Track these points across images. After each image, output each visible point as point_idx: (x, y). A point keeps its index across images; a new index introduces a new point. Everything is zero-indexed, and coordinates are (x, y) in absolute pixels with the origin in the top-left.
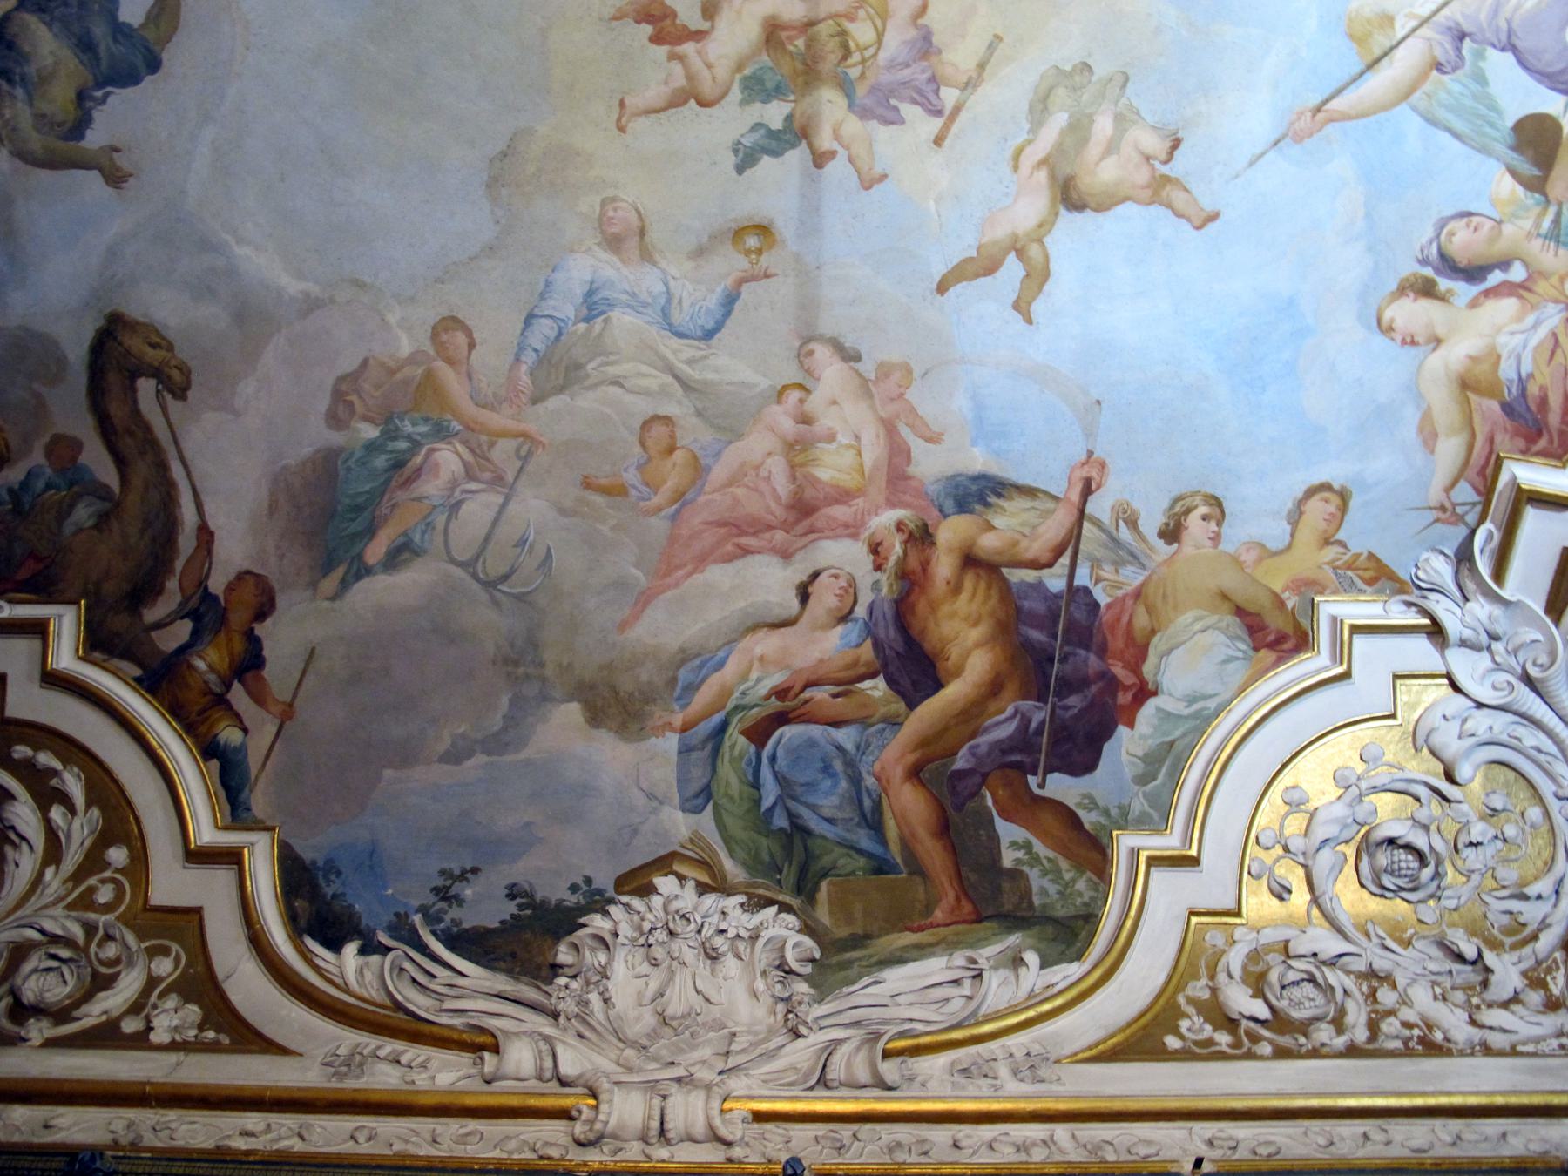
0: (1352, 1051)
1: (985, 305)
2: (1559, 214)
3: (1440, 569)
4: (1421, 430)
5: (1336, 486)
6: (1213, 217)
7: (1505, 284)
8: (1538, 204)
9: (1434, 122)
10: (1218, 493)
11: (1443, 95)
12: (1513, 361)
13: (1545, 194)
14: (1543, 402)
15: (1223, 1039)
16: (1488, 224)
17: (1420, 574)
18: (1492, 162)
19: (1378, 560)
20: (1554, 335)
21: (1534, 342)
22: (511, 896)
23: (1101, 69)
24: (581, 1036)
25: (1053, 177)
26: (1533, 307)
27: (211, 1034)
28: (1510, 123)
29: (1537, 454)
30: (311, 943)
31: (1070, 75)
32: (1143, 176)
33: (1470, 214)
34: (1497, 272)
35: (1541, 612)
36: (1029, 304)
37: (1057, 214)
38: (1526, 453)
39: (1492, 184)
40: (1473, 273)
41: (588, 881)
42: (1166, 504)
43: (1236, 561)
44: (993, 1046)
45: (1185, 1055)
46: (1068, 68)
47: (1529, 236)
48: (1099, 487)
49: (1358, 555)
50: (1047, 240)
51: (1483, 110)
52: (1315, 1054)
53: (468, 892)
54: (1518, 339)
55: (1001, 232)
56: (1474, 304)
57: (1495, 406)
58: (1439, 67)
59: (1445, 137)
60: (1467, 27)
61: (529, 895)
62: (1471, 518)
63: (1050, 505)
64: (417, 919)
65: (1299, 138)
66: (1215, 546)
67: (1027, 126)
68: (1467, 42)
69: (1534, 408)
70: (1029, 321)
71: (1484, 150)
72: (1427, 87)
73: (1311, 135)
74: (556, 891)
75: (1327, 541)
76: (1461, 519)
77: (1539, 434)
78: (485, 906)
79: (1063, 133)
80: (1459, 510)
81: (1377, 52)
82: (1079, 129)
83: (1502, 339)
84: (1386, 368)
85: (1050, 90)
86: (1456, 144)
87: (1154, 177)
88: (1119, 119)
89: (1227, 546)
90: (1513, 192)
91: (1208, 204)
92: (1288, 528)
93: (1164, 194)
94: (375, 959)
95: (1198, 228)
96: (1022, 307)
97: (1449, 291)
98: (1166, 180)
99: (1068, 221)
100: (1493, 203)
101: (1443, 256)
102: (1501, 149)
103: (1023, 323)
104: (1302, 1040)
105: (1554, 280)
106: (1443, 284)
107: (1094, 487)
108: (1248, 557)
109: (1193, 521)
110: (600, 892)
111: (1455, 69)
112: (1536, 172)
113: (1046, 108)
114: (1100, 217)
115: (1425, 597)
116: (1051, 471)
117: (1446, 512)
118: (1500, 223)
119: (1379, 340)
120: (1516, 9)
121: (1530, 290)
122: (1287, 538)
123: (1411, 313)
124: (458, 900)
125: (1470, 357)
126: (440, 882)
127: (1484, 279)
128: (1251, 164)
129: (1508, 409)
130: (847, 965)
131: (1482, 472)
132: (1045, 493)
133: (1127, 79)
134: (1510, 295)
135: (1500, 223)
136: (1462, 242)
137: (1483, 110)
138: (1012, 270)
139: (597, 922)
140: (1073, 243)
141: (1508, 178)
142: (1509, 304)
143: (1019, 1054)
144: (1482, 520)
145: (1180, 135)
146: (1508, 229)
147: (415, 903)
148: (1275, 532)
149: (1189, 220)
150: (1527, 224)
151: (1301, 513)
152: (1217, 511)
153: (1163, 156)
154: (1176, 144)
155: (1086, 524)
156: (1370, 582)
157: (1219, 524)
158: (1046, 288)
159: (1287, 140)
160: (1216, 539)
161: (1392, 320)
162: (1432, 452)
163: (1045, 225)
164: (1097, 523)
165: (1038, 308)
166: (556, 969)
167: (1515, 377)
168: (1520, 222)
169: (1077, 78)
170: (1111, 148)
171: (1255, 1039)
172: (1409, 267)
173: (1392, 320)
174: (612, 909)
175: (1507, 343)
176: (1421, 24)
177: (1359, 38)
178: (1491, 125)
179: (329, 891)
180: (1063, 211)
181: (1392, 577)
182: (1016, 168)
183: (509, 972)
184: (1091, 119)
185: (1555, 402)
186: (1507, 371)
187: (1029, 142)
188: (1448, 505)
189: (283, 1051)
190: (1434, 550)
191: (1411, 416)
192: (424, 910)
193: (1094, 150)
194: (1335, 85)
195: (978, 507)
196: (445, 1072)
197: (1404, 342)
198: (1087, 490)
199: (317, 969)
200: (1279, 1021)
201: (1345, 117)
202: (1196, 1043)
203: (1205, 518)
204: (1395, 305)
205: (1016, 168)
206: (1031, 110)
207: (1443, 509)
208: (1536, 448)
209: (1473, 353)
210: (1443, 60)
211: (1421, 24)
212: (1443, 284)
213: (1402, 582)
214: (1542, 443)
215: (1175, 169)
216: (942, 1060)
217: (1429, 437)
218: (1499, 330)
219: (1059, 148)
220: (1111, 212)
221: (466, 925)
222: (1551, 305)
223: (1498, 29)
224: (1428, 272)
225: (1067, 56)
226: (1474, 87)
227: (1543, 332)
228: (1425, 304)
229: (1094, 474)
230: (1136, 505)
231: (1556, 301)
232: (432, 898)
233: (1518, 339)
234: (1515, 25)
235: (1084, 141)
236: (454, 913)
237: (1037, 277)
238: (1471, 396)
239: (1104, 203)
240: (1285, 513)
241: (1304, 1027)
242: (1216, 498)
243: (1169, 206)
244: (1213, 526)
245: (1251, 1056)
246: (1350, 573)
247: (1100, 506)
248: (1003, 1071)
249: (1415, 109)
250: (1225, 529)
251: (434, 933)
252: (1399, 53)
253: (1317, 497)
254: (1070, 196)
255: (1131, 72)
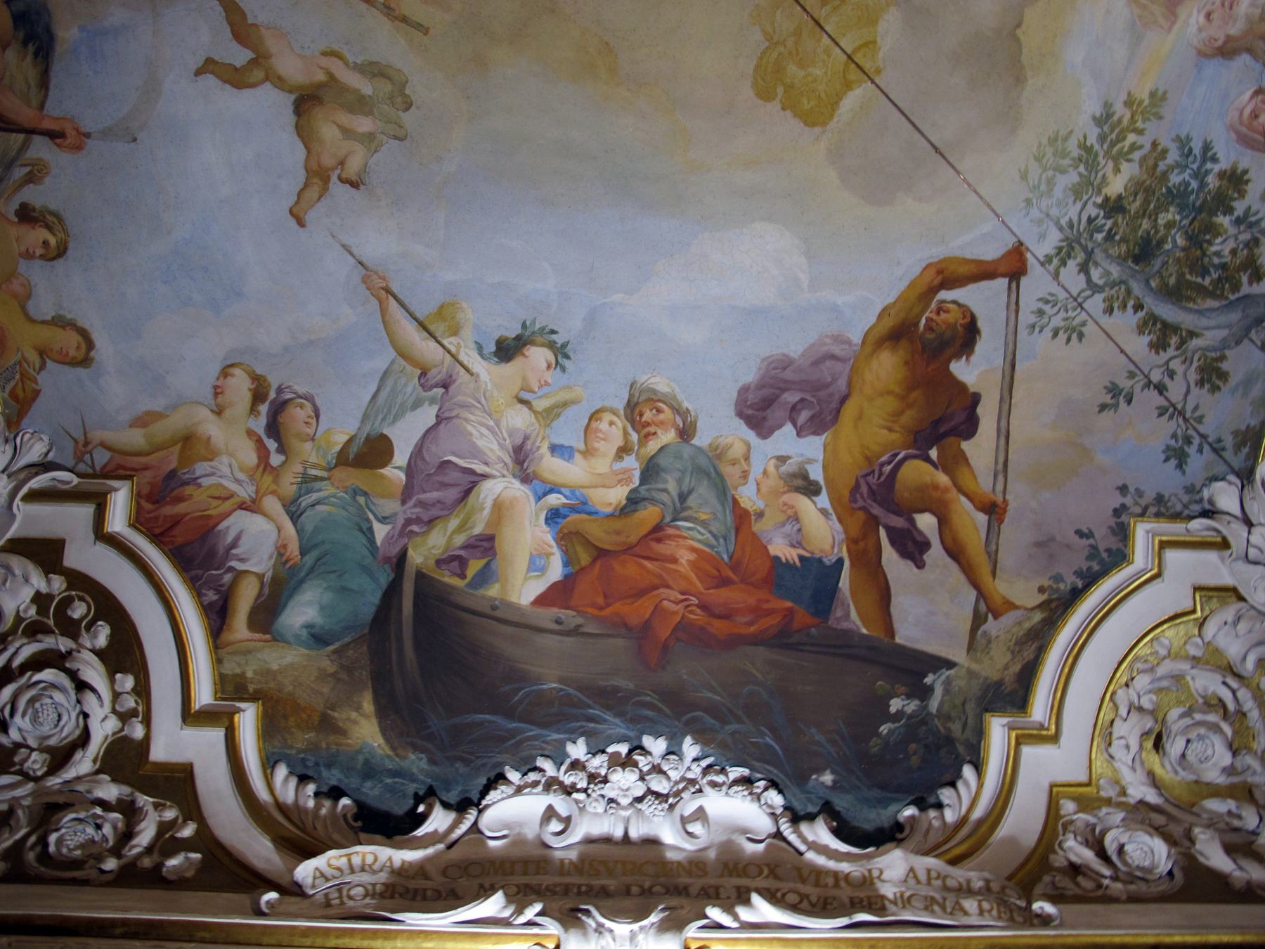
1: (206, 34)
2: (322, 479)
3: (35, 452)
4: (148, 413)
5: (93, 354)
6: (301, 223)
7: (268, 452)
8: (328, 463)
9: (385, 375)
10: (69, 252)
11: (403, 381)
12: (209, 470)
13: (336, 466)
14: (180, 499)
16: (310, 431)
17: (28, 436)
18: (357, 425)
19: (34, 399)
20: (232, 496)
21: (225, 482)
23: (407, 118)
25: (321, 86)
26: (251, 477)
28: (385, 432)
29: (138, 504)
31: (403, 94)
32: (328, 161)
33: (317, 417)
34: (276, 445)
35: (9, 535)
36: (213, 73)
37: (290, 92)
38: (139, 498)
39: (342, 426)
40: (274, 428)
42: (53, 207)
43: (12, 275)
46: (407, 92)
47: (304, 462)
48: (58, 145)
49: (36, 383)
50: (268, 84)
51: (393, 412)
54: (226, 470)
55: (272, 44)
56: (250, 433)
57: (173, 466)
58: (424, 374)
59: (373, 388)
60: (452, 389)
62: (82, 467)
63: (35, 103)
65: (365, 280)
66: (20, 255)
67: (359, 62)
68: (442, 390)
69: (175, 493)
70: (198, 73)
71: (365, 417)
72: (409, 368)
73: (368, 289)
75: (43, 353)
76: (79, 459)
77: (153, 503)
79: (356, 91)
80: (87, 457)
81: (432, 328)
82: (361, 105)
83: (225, 459)
84: (193, 375)
85: (389, 78)
86: (369, 397)
87: (328, 170)
88: (371, 136)
89: (23, 266)
90: (336, 443)
91: (310, 217)
92: (49, 318)
93: (316, 180)
95: (291, 211)
96: (209, 67)
97: (259, 413)
98: (326, 180)
99: (286, 102)
100: (328, 431)
101: (286, 402)
102: (367, 429)
103: (195, 68)
105: (273, 487)
106: (264, 408)
107: (58, 141)
108: (16, 286)
109: (42, 234)
111: (422, 385)
112: (351, 457)
113: (374, 75)
114: (292, 129)
115: (7, 441)
116: (65, 101)
117: (84, 447)
118: (313, 439)
119: (215, 369)
120: (466, 420)
121: (264, 470)
122: (41, 318)
123: (240, 386)
125: (209, 439)
127: (269, 437)
128: (343, 246)
129: (172, 474)
131: (120, 467)
132: (46, 96)
133: (401, 140)
134: (259, 458)
135: (313, 439)
136: (298, 415)
137: (393, 412)
138: (239, 56)
140: (267, 107)
141: (346, 438)
142: (251, 458)
144: (78, 475)
145: (362, 187)
146: (308, 446)
148: (44, 306)
149: (297, 203)
150: (313, 459)
151: (63, 327)
152: (55, 253)
153: (344, 176)
154: (354, 185)
155: (22, 137)
156: (13, 395)
157: (42, 257)
158: (228, 87)
159: (364, 271)
160: (28, 255)
161: (232, 375)
162: (131, 426)
163: (280, 83)
164: (24, 147)
165: (210, 81)
167: (197, 474)
168: (314, 453)
169: (399, 100)
170: (347, 133)
172: (274, 381)
173: (232, 375)
175: (222, 464)
176: (452, 356)
177: (443, 312)
178: (384, 419)
180: (293, 97)
181: (21, 414)
182: (324, 54)
184: (369, 113)
185: (181, 508)
186: (201, 468)
187: (347, 64)
188: (90, 447)
190: (51, 445)
191: (158, 405)
193: (345, 118)
194: (406, 301)
195: (21, 35)
197: (216, 387)
198: (54, 136)
201: (383, 311)
203: (46, 243)
204: (244, 375)
205: (324, 54)
206: (372, 63)
207: (86, 444)
208: (143, 503)
209: (213, 440)
210: (429, 375)
211: (452, 356)
212: (264, 408)
213: (19, 422)
214: (147, 506)
215: (336, 188)
217: (142, 421)
218: (231, 455)
219: (343, 89)
220: (296, 138)
222: (254, 488)
223: (451, 410)
224: (272, 395)
225: (416, 89)
226: (411, 401)
227: (233, 487)
228: (247, 397)
229: (69, 141)
230: (47, 180)
231: (257, 492)
233: (226, 470)
234: (456, 421)
235: (351, 110)
237: (236, 78)
238: (179, 446)
239: (304, 131)
240: (62, 312)
242: (65, 250)
243: (306, 185)
244: (39, 252)
246: (18, 376)
247: (41, 149)
249: (392, 362)
250: (38, 263)
252: (433, 344)
253: (80, 339)
254: (306, 102)
255: (407, 142)
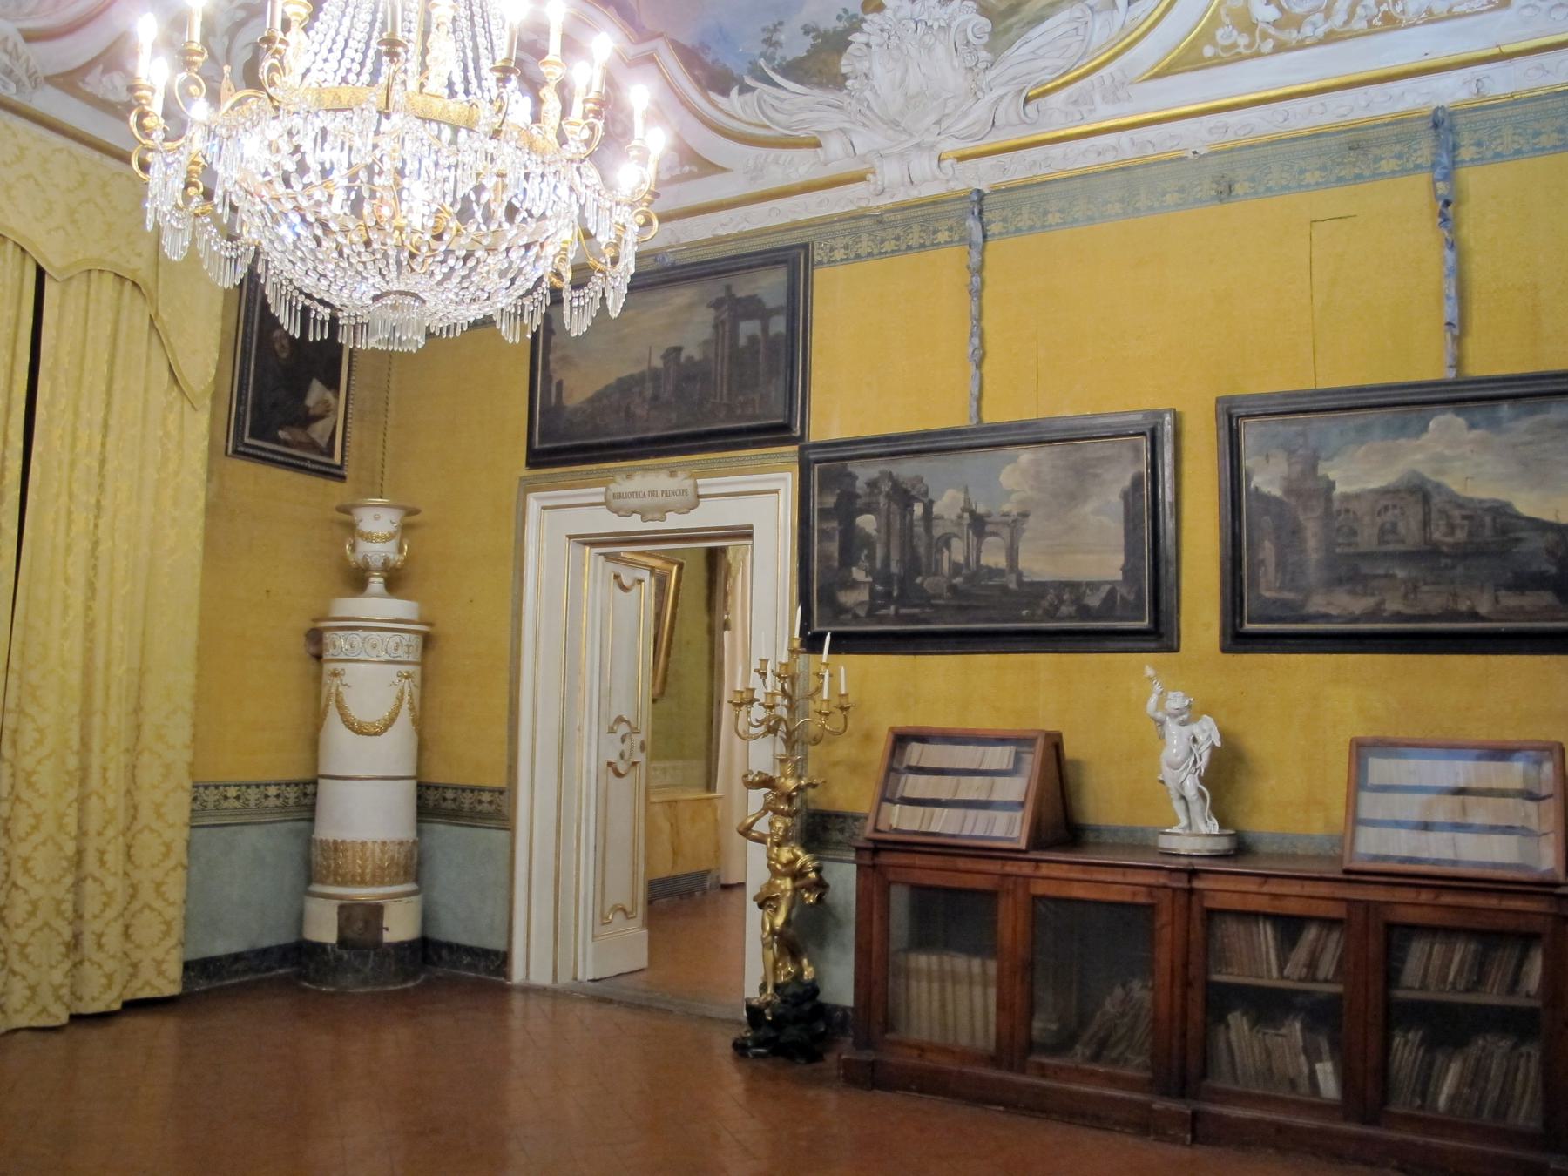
0: (1330, 38)
15: (1243, 41)
22: (807, 33)
24: (865, 125)
27: (687, 169)
30: (713, 95)
41: (845, 11)
44: (1093, 77)
45: (1218, 62)
52: (1301, 46)
53: (783, 38)
61: (816, 29)
64: (762, 62)
74: (830, 24)
78: (796, 46)
94: (748, 96)
104: (1294, 34)
110: (855, 16)
124: (776, 44)
126: (765, 36)
130: (1008, 30)
139: (857, 38)
143: (1108, 82)
147: (757, 52)
166: (845, 77)
171: (1265, 36)
174: (864, 26)
179: (709, 59)
183: (820, 85)
189: (724, 170)
192: (762, 55)
196: (801, 165)
199: (721, 110)
200: (1289, 20)
202: (1226, 49)
216: (1063, 94)
221: (789, 58)
232: (764, 47)
236: (779, 53)
241: (1298, 22)
245: (1258, 55)
248: (1097, 98)
251: (774, 70)
